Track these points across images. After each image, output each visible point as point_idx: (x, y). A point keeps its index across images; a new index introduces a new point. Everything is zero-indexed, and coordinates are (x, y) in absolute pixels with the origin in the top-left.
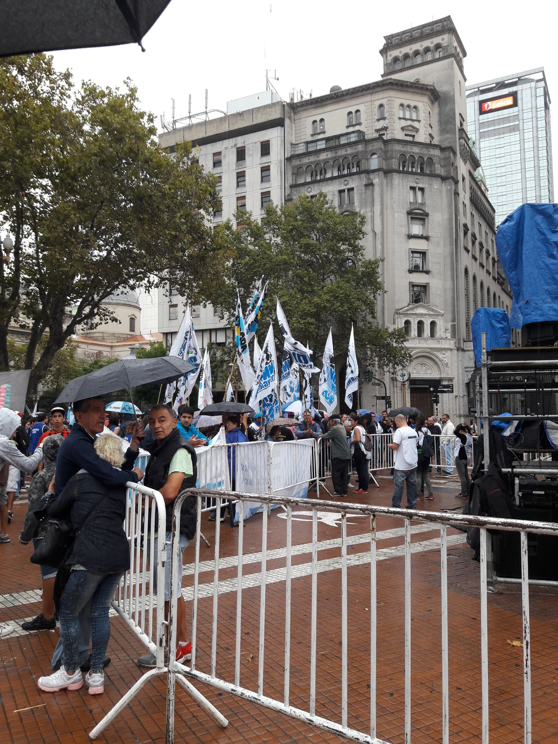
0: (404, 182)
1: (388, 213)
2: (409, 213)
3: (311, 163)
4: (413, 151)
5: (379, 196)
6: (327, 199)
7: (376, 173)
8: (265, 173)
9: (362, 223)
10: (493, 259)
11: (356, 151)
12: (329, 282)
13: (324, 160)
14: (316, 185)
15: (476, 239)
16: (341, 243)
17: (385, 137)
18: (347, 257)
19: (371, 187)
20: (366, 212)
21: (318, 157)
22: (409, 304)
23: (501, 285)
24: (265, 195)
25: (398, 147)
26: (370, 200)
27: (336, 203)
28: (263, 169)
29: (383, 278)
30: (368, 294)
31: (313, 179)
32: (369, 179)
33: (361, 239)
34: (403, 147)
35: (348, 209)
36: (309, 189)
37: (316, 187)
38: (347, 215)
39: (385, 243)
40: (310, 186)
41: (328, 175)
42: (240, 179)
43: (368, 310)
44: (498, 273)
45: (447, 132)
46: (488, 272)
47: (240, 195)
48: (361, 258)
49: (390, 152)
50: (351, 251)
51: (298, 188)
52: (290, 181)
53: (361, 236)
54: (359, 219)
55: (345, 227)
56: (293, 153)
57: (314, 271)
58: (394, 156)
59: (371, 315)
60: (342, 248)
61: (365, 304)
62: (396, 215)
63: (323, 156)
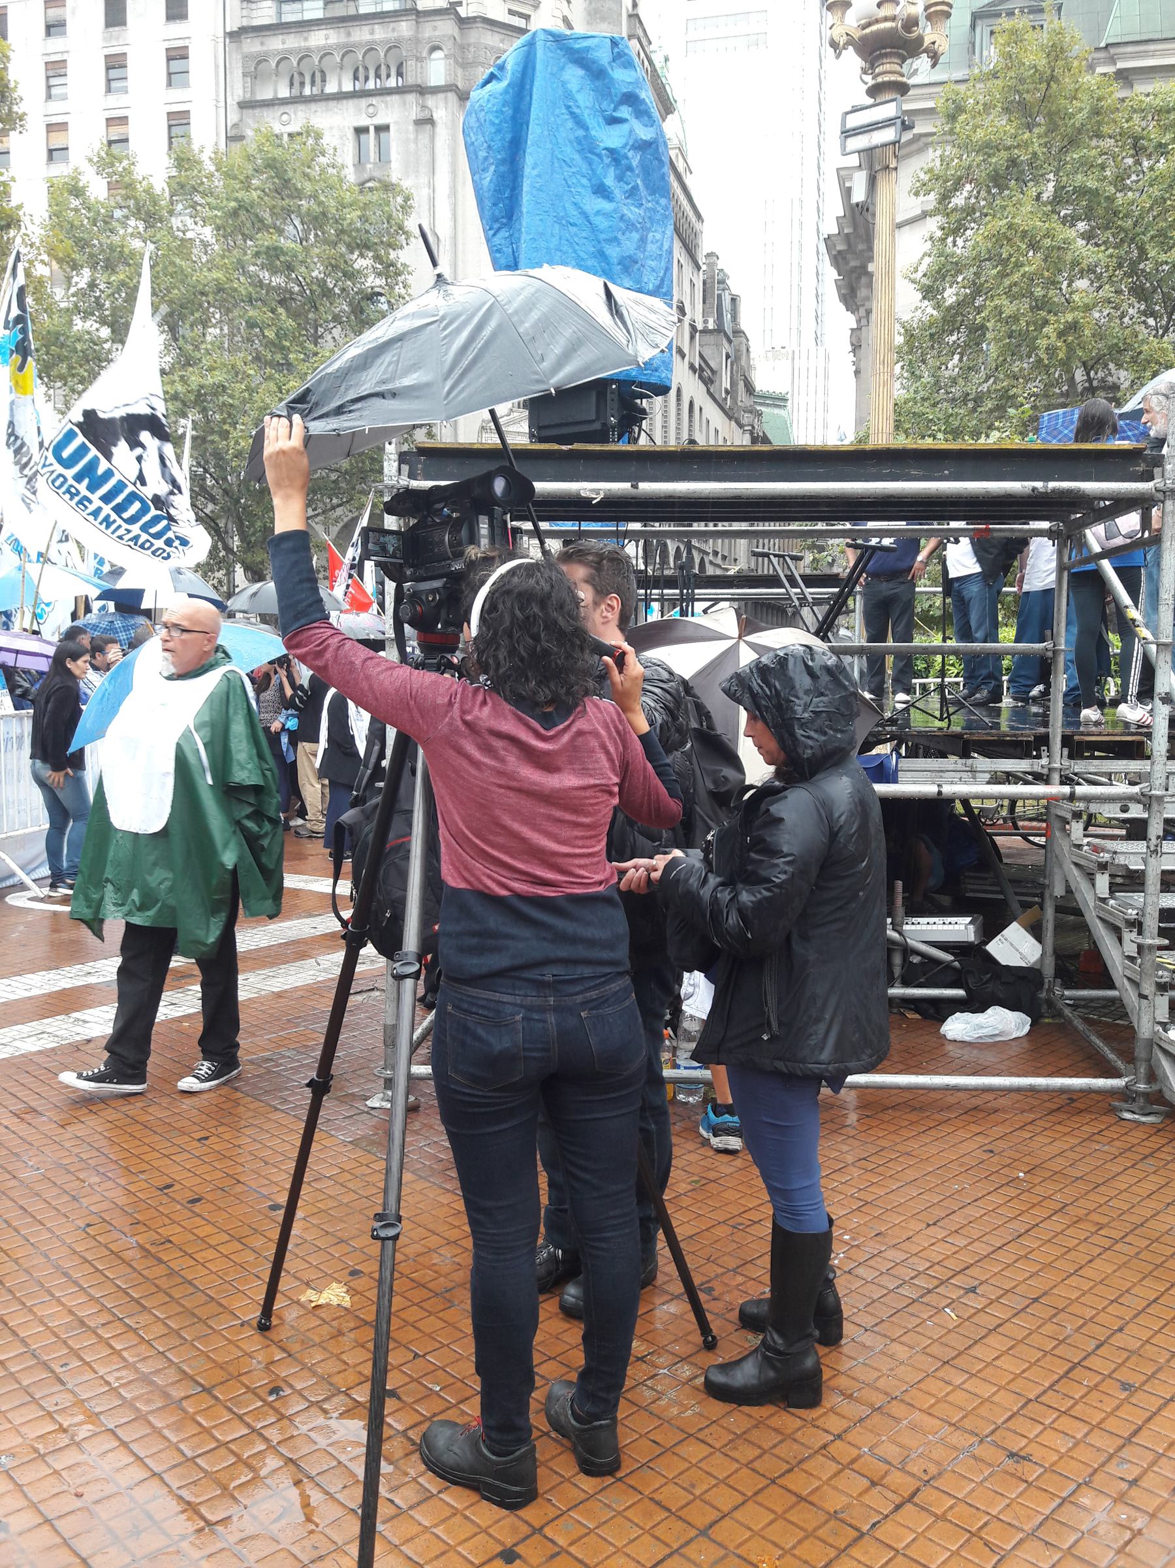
3: (291, 51)
5: (447, 151)
6: (324, 142)
7: (441, 96)
9: (406, 208)
11: (395, 34)
12: (331, 344)
13: (319, 49)
14: (301, 107)
16: (357, 253)
17: (463, 12)
18: (372, 288)
19: (429, 127)
21: (306, 39)
23: (706, 384)
24: (178, 120)
25: (492, 39)
27: (347, 156)
28: (173, 53)
31: (296, 91)
32: (424, 107)
33: (401, 247)
34: (502, 41)
35: (376, 174)
36: (285, 117)
37: (300, 113)
38: (371, 190)
39: (460, 263)
41: (331, 88)
42: (114, 73)
44: (701, 356)
45: (603, 19)
47: (114, 114)
48: (403, 291)
49: (472, 49)
50: (379, 274)
51: (257, 111)
52: (238, 92)
58: (482, 60)
63: (318, 39)
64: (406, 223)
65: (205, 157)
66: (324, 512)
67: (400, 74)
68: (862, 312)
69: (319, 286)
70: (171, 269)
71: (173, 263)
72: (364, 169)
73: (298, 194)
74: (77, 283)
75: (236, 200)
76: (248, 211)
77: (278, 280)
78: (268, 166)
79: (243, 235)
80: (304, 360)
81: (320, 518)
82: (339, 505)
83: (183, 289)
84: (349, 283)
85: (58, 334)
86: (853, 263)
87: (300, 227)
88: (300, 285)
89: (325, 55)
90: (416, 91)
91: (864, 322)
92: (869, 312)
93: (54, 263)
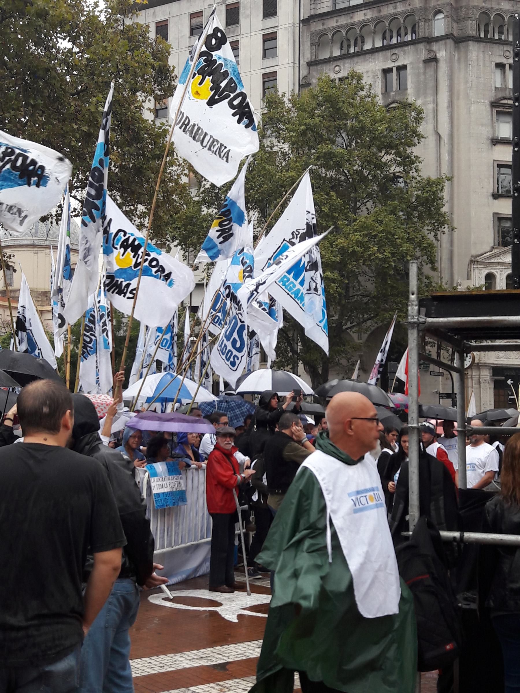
0: (487, 56)
1: (461, 104)
2: (494, 105)
3: (341, 27)
4: (502, 7)
5: (446, 78)
6: (363, 82)
7: (443, 42)
8: (269, 44)
9: (418, 119)
11: (411, 7)
12: (365, 213)
13: (361, 22)
14: (347, 61)
18: (394, 173)
19: (433, 64)
20: (425, 104)
21: (352, 18)
22: (493, 248)
26: (431, 84)
27: (378, 89)
29: (452, 207)
30: (425, 231)
31: (344, 52)
32: (430, 51)
33: (415, 145)
35: (397, 98)
36: (337, 68)
37: (347, 65)
38: (394, 108)
39: (455, 152)
40: (338, 63)
41: (368, 46)
43: (425, 257)
48: (415, 174)
50: (399, 164)
51: (319, 67)
52: (307, 56)
53: (416, 140)
54: (413, 114)
55: (389, 127)
56: (312, 12)
57: (340, 195)
58: (470, 15)
59: (430, 265)
60: (383, 160)
61: (420, 246)
62: (472, 109)
63: (359, 16)
64: (418, 129)
65: (286, 100)
66: (358, 324)
67: (414, 32)
69: (358, 175)
70: (263, 172)
71: (264, 168)
72: (389, 96)
73: (346, 116)
74: (205, 185)
75: (305, 124)
76: (312, 131)
77: (330, 174)
78: (326, 101)
79: (309, 146)
80: (347, 225)
81: (355, 329)
82: (368, 319)
83: (270, 184)
84: (378, 172)
85: (192, 217)
87: (346, 138)
88: (345, 175)
89: (364, 26)
90: (425, 41)
93: (191, 174)
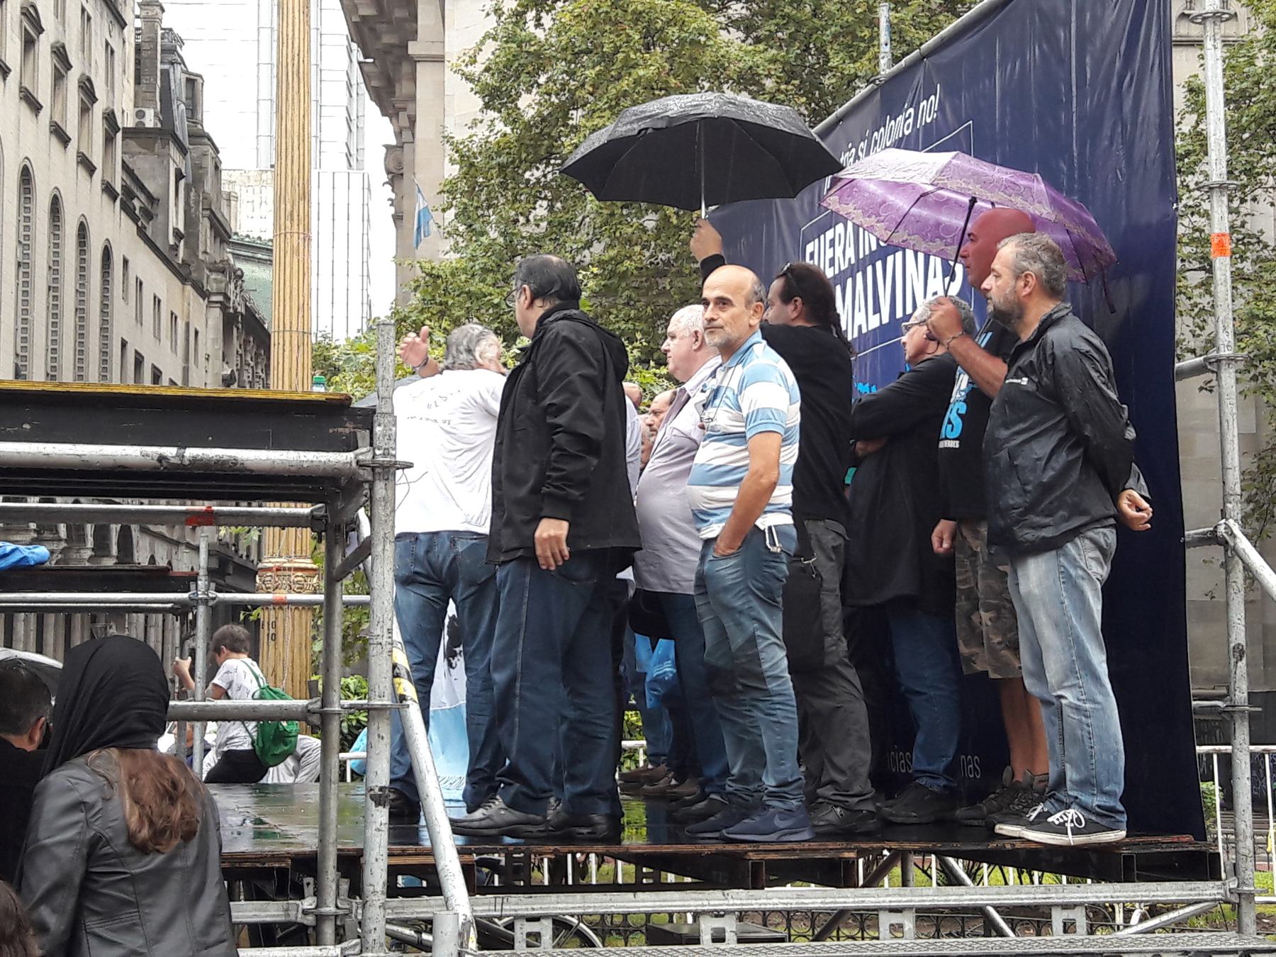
10: (110, 117)
15: (40, 30)
46: (85, 163)
68: (403, 117)
86: (388, 39)
91: (406, 136)
92: (412, 121)
